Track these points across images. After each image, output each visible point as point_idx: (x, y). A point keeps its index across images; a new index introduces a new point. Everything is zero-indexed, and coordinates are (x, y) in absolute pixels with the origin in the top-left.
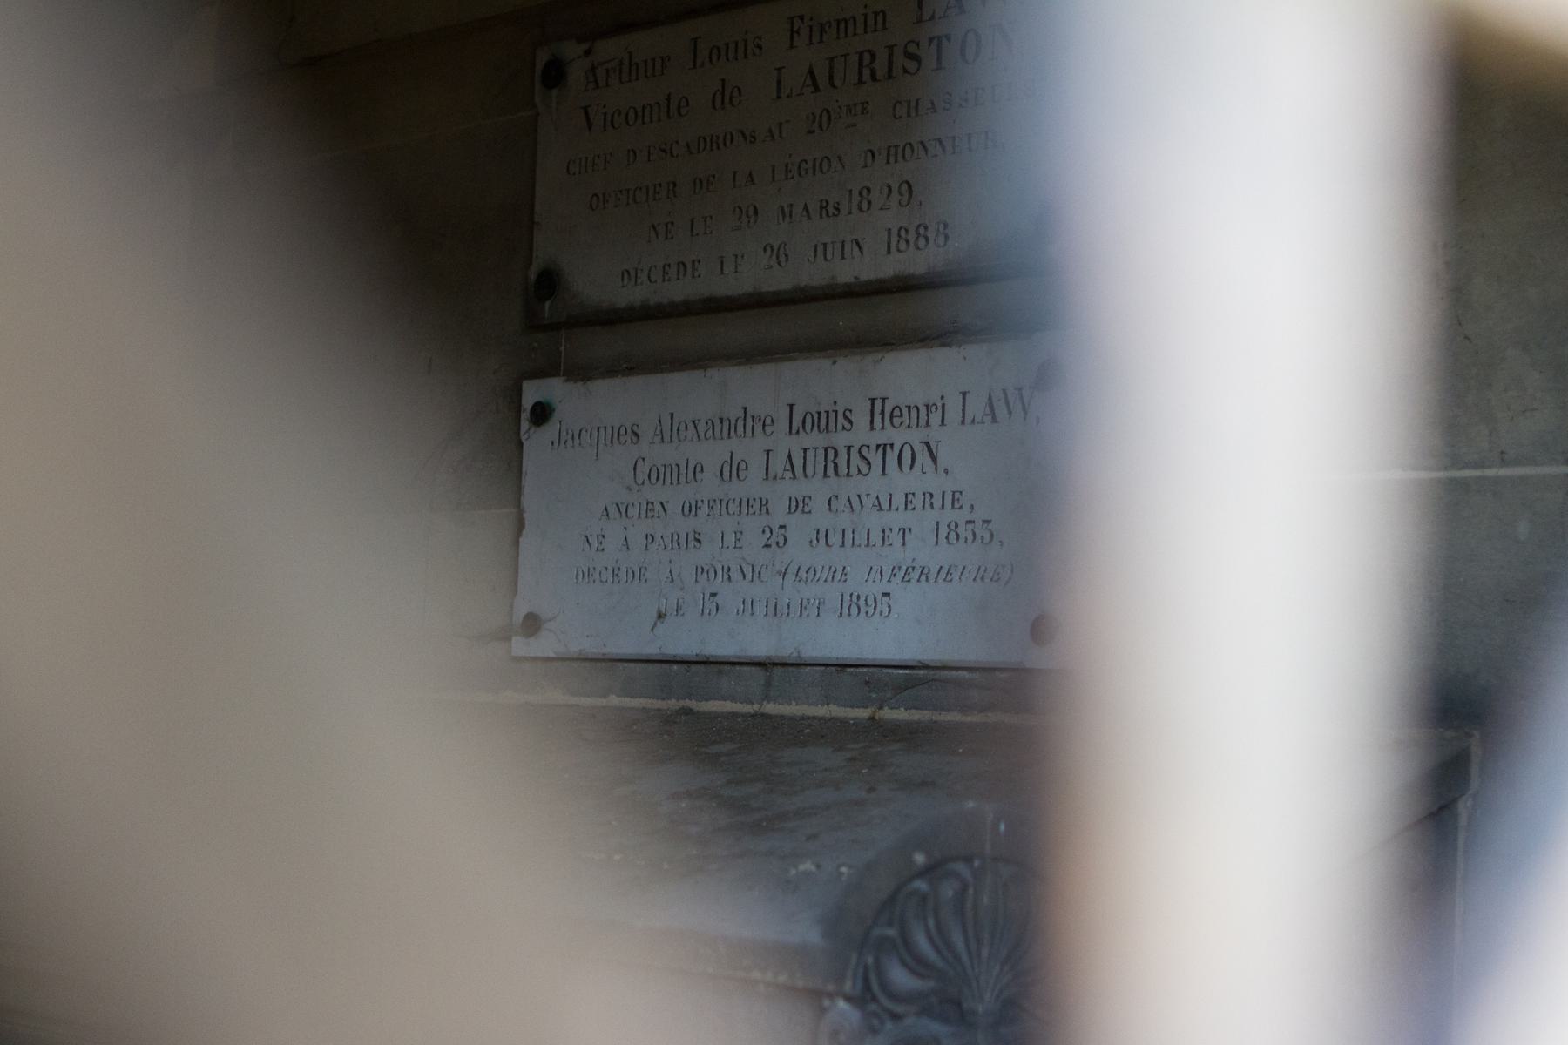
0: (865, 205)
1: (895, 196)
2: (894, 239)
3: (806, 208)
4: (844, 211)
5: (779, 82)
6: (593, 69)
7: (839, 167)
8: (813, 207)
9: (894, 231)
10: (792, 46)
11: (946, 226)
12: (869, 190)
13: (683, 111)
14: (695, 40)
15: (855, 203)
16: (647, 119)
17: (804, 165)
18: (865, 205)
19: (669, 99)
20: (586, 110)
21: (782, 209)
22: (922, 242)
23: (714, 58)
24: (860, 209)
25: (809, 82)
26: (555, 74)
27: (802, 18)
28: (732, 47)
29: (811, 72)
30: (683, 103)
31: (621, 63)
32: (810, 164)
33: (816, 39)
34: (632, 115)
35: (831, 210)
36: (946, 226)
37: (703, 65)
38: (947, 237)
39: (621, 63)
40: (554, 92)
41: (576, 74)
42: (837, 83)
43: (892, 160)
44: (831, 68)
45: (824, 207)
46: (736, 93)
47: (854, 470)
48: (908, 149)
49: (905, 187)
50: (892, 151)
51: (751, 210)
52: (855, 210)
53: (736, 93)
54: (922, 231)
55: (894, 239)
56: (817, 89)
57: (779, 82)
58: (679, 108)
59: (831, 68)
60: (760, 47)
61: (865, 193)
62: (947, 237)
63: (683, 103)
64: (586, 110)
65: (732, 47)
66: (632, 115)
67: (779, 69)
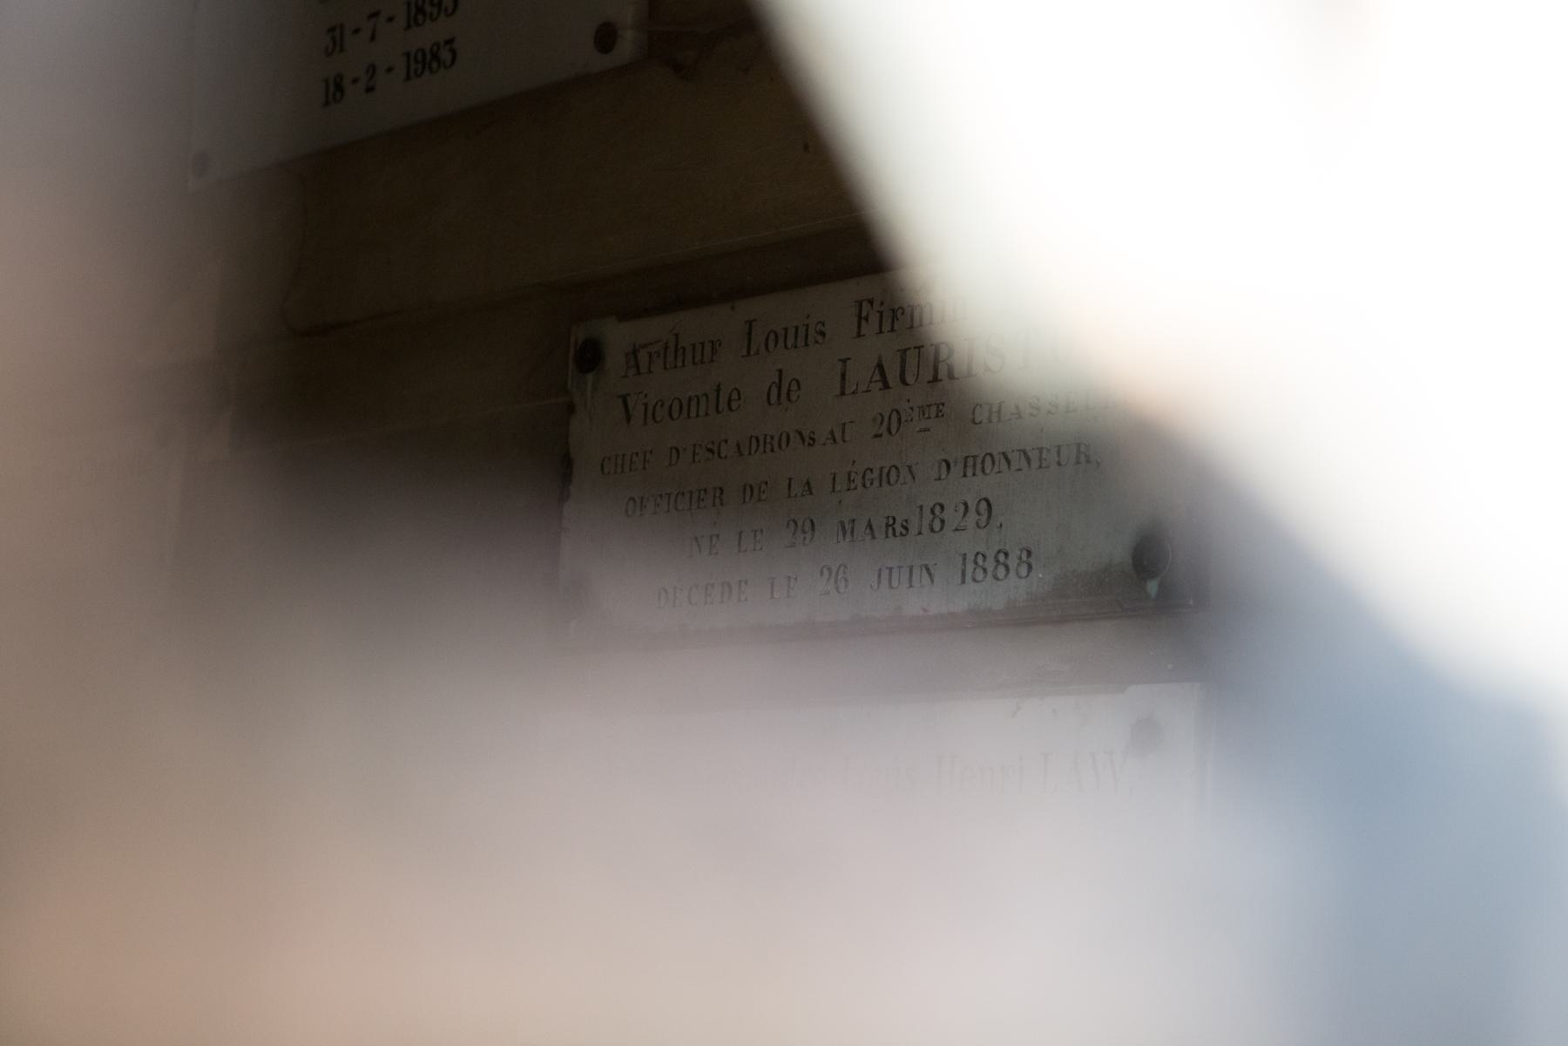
0: (937, 526)
1: (972, 516)
2: (970, 567)
3: (870, 526)
4: (913, 530)
5: (843, 376)
6: (635, 352)
7: (909, 477)
8: (879, 523)
9: (970, 557)
10: (859, 335)
11: (1029, 553)
12: (942, 507)
13: (734, 405)
14: (750, 323)
15: (926, 523)
16: (693, 414)
17: (869, 475)
18: (937, 526)
19: (718, 391)
20: (624, 399)
21: (842, 523)
22: (1001, 571)
23: (771, 344)
24: (932, 530)
25: (877, 377)
26: (591, 357)
27: (871, 302)
28: (791, 333)
29: (880, 367)
30: (735, 396)
31: (666, 348)
32: (876, 474)
33: (886, 326)
35: (899, 529)
36: (1029, 553)
37: (757, 353)
38: (1030, 567)
39: (666, 348)
40: (590, 377)
41: (615, 358)
42: (910, 379)
43: (970, 472)
44: (903, 361)
45: (890, 525)
46: (794, 387)
48: (988, 460)
49: (984, 505)
50: (970, 461)
51: (808, 524)
52: (925, 530)
53: (794, 387)
54: (1002, 558)
55: (970, 567)
56: (886, 386)
57: (843, 376)
58: (730, 400)
59: (903, 361)
60: (823, 334)
61: (938, 509)
62: (1030, 567)
63: (735, 396)
64: (624, 399)
65: (791, 333)
67: (844, 361)
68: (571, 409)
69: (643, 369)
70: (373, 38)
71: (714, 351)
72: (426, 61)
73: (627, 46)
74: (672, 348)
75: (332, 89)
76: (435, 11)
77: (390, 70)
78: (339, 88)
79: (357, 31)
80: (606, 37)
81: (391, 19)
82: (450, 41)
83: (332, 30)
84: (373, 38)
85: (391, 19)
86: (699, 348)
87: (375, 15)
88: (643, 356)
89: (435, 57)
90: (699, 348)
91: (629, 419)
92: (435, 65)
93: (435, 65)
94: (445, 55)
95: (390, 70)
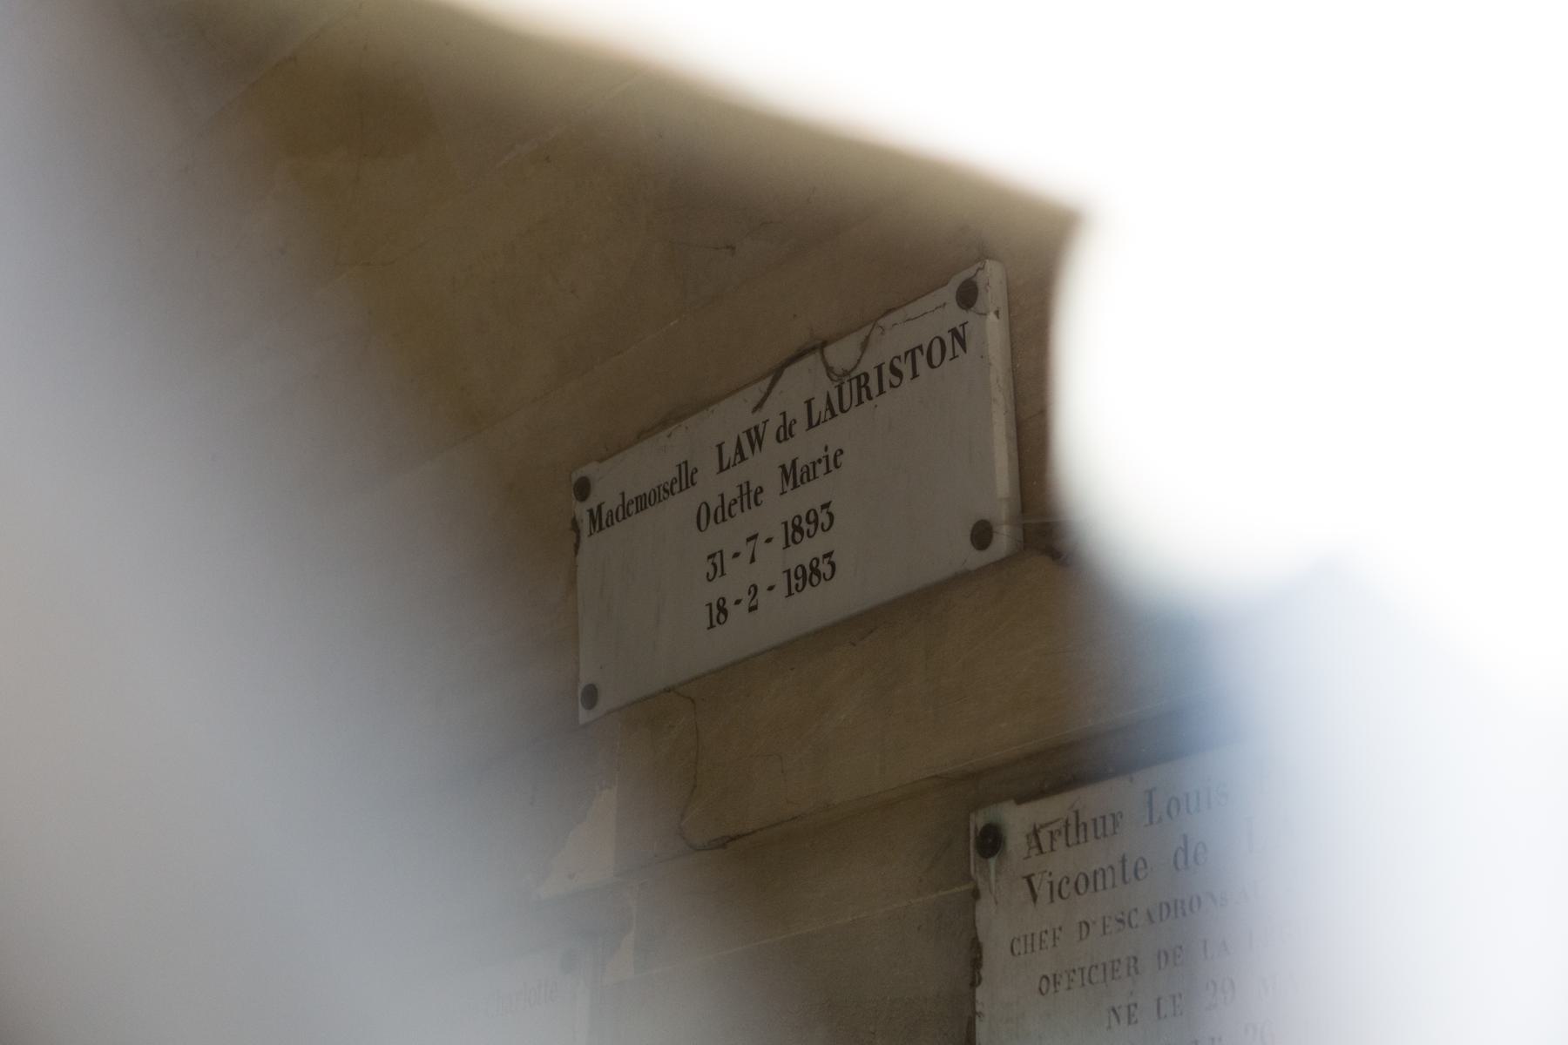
6: (1036, 833)
13: (1141, 875)
16: (1100, 887)
19: (1123, 861)
20: (1029, 879)
26: (991, 841)
30: (1141, 865)
31: (1067, 825)
34: (1082, 882)
37: (1160, 819)
39: (1067, 825)
40: (992, 861)
41: (1016, 840)
47: (886, 386)
63: (1141, 865)
64: (1029, 879)
66: (1082, 882)
68: (976, 894)
69: (1046, 847)
70: (753, 560)
71: (1115, 824)
72: (808, 576)
73: (1003, 542)
74: (1072, 822)
75: (715, 612)
76: (812, 527)
77: (771, 588)
78: (723, 610)
79: (736, 555)
80: (982, 535)
81: (769, 540)
82: (829, 555)
83: (712, 556)
84: (753, 560)
85: (769, 540)
86: (1100, 822)
87: (755, 537)
88: (1044, 836)
89: (815, 571)
90: (1100, 822)
91: (1035, 898)
92: (815, 579)
93: (815, 579)
94: (824, 568)
95: (771, 588)
